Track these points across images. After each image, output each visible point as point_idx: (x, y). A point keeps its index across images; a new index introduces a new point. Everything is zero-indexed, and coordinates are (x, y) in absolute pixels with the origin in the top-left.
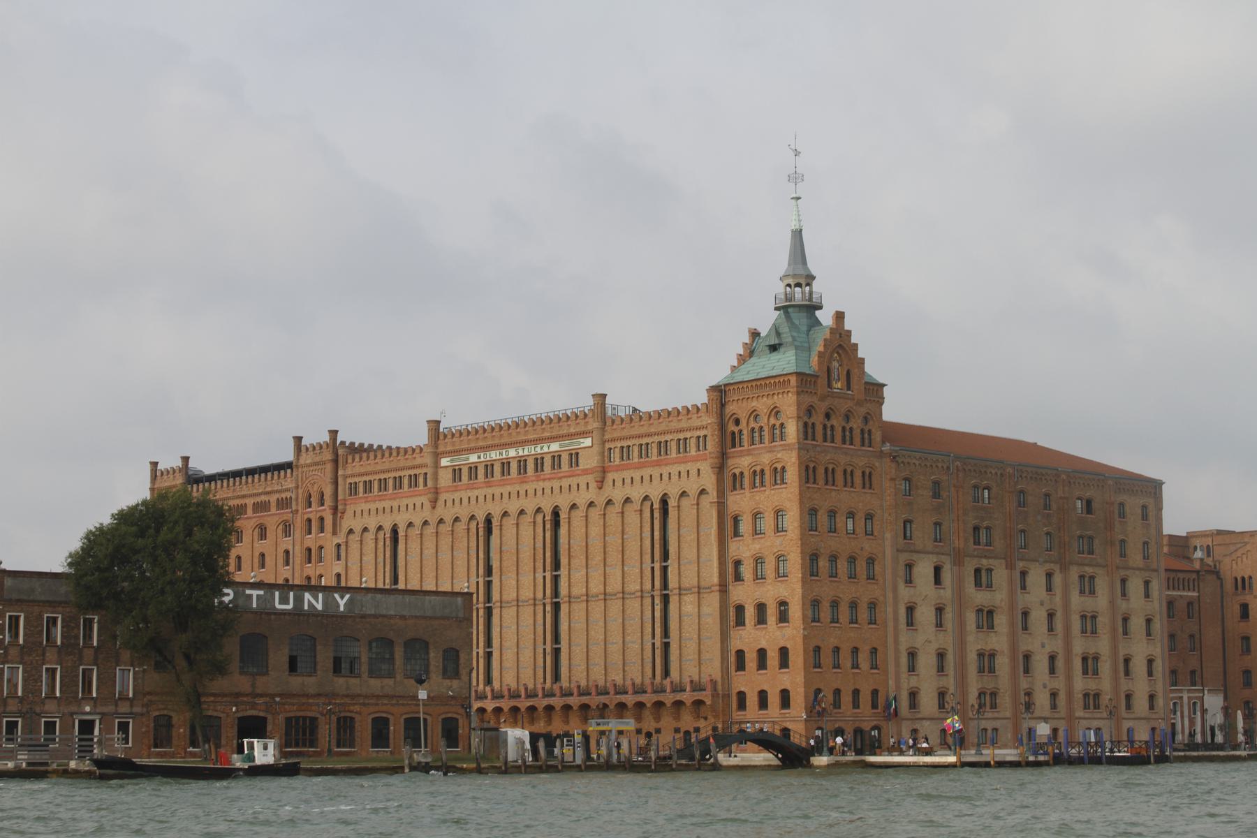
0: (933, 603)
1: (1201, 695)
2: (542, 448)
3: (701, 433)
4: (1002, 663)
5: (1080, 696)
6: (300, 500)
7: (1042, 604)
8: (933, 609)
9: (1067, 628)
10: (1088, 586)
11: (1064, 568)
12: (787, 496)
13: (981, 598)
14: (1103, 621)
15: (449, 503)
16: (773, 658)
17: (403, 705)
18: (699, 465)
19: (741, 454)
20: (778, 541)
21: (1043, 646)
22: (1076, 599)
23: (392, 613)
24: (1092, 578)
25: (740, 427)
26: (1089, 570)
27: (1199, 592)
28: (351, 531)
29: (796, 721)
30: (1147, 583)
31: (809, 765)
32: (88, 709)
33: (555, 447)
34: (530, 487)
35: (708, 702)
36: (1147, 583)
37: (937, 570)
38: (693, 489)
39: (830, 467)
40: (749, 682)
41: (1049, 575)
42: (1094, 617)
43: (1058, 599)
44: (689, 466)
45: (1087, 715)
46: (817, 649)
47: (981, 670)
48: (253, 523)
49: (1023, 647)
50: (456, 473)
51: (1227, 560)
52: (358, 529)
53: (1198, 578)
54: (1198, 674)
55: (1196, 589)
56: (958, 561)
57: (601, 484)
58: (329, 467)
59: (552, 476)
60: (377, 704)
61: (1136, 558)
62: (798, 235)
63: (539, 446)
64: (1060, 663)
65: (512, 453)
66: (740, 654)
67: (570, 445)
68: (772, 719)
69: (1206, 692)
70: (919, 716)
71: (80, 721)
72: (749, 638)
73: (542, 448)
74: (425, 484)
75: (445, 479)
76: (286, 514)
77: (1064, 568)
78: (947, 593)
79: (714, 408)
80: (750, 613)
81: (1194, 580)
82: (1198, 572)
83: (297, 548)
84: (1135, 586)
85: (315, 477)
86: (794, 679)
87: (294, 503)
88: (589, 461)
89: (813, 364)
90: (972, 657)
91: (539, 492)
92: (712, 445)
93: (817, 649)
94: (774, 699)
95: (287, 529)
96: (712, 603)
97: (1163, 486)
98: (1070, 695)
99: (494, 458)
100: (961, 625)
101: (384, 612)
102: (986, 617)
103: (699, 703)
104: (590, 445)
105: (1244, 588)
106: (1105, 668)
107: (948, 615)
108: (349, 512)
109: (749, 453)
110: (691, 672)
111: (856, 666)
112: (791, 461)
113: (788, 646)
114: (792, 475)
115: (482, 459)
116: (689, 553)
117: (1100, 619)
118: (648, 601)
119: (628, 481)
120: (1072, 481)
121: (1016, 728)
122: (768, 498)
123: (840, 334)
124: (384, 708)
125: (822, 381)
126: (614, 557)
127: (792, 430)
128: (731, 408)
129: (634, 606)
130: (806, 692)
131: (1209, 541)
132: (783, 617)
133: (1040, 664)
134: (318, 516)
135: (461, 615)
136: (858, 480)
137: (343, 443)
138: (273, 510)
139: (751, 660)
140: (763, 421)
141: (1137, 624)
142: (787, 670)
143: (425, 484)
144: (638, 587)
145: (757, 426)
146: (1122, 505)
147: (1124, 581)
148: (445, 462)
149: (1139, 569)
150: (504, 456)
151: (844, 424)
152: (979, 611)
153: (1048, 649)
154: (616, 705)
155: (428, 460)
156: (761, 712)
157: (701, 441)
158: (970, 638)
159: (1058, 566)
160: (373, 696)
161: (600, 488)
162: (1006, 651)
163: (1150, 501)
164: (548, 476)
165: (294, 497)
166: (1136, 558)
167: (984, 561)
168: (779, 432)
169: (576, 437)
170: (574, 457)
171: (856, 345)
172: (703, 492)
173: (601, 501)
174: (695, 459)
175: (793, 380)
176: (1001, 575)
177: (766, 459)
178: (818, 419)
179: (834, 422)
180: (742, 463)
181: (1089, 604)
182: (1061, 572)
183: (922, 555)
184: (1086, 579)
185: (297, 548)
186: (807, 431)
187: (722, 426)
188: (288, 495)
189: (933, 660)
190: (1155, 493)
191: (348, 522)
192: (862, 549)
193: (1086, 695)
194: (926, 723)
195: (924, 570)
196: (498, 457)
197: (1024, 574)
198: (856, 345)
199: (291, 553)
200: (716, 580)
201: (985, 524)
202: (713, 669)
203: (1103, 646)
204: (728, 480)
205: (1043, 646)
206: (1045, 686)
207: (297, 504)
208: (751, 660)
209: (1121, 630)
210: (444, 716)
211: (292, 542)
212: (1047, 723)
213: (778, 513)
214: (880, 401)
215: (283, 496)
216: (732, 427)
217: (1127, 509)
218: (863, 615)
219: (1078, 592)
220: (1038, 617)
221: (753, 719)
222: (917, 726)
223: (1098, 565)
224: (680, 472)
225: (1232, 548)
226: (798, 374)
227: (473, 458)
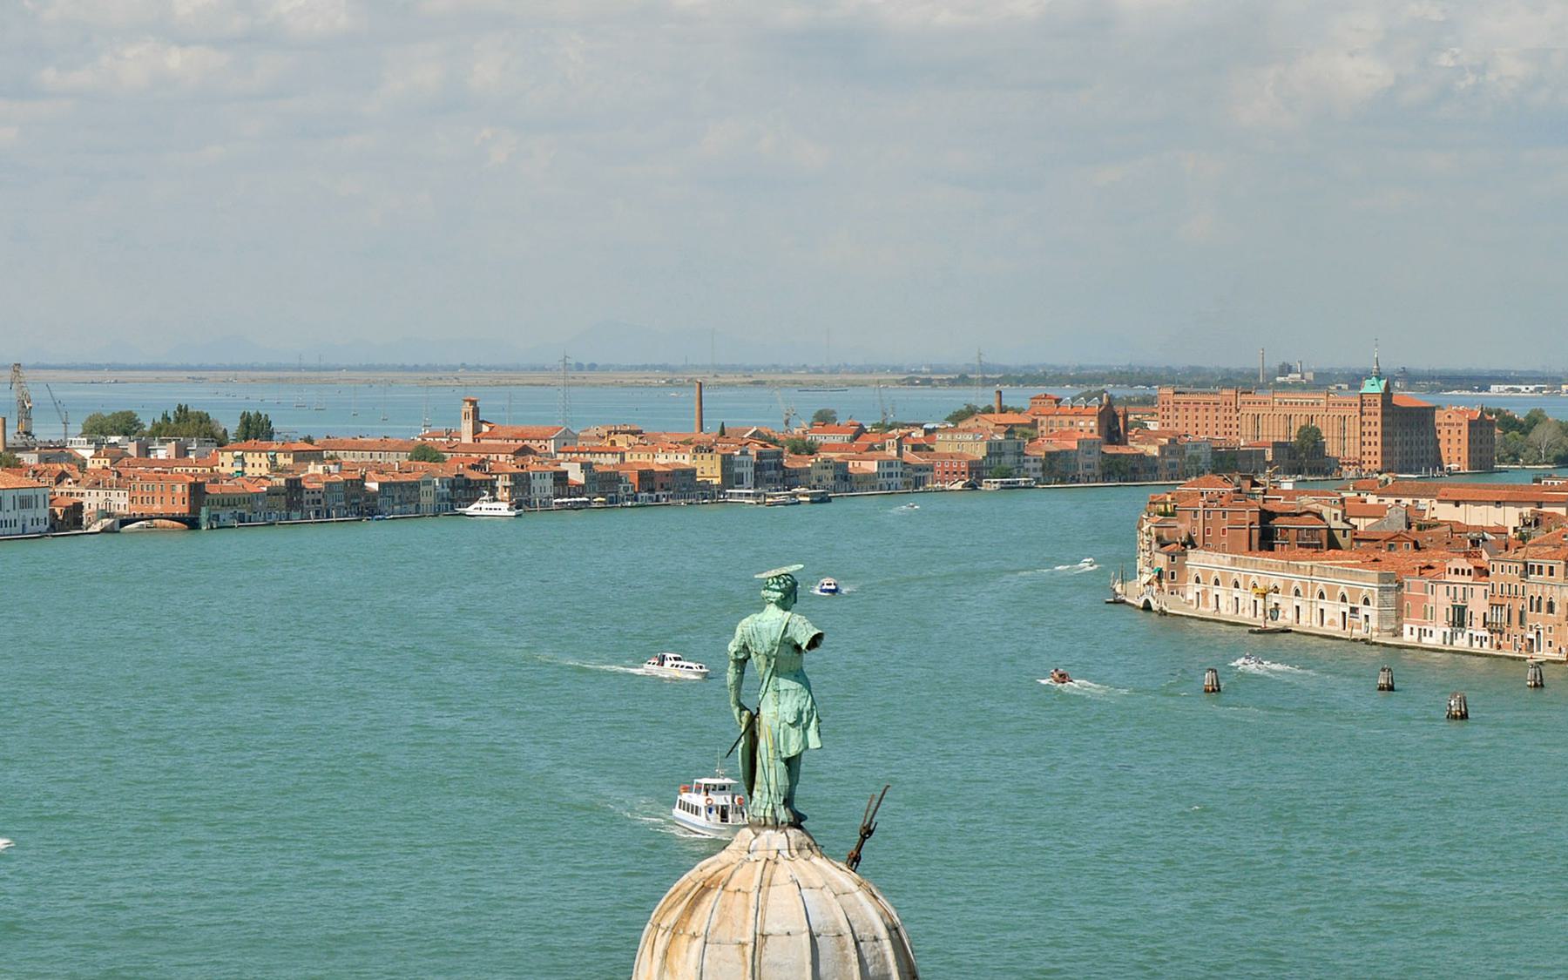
12: (1378, 419)
50: (1280, 403)
52: (1245, 413)
75: (1276, 404)
92: (1359, 406)
94: (1373, 462)
114: (1379, 414)
122: (1372, 419)
127: (1379, 405)
129: (1335, 440)
168: (1376, 405)
204: (1362, 414)
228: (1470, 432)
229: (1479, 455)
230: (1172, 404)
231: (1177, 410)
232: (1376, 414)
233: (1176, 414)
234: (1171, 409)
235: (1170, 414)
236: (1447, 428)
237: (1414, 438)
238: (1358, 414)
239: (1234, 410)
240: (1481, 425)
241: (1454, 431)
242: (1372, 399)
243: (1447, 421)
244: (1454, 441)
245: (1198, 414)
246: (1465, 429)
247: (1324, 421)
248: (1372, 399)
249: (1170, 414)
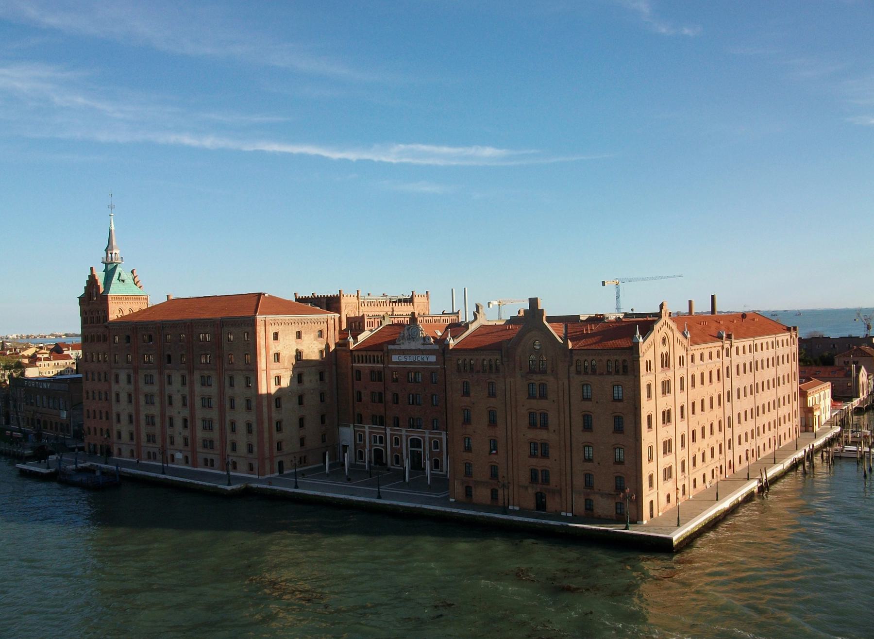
5: (201, 441)
10: (205, 382)
11: (191, 373)
13: (147, 389)
21: (179, 413)
22: (198, 388)
24: (209, 377)
37: (129, 376)
41: (183, 377)
47: (148, 424)
62: (110, 231)
90: (142, 417)
100: (137, 403)
147: (231, 378)
149: (241, 370)
152: (146, 395)
181: (207, 391)
189: (127, 418)
195: (123, 377)
197: (169, 377)
205: (179, 413)
206: (180, 434)
212: (181, 452)
219: (199, 385)
220: (177, 399)
222: (120, 447)
237: (176, 388)
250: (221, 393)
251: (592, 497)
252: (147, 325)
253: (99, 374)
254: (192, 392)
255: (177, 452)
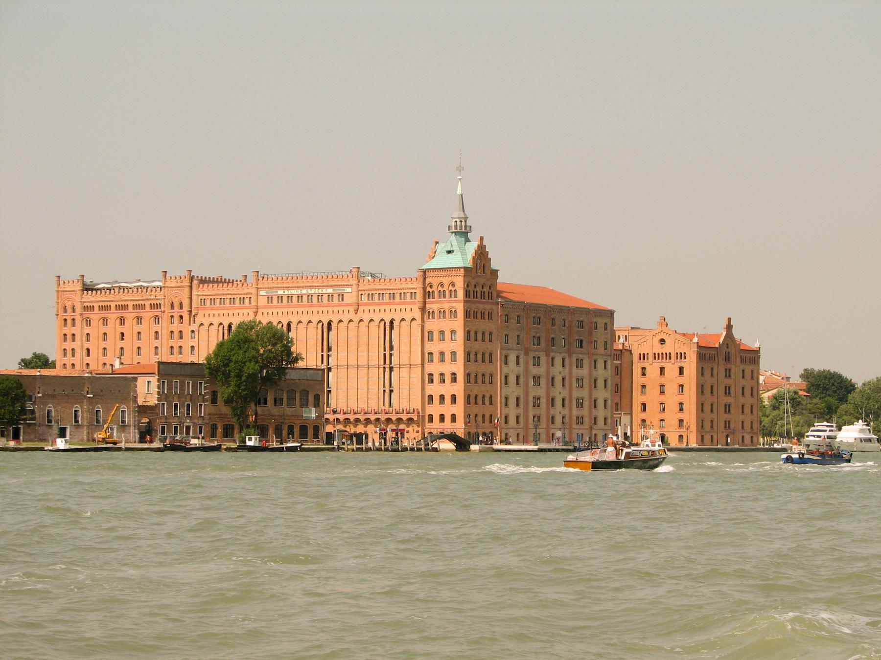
0: (516, 373)
1: (620, 416)
2: (322, 291)
3: (413, 291)
4: (543, 401)
6: (166, 305)
7: (560, 373)
8: (515, 376)
9: (571, 384)
11: (570, 355)
12: (458, 324)
13: (534, 371)
14: (586, 381)
15: (265, 314)
16: (448, 399)
17: (299, 419)
18: (412, 306)
19: (432, 303)
20: (452, 345)
21: (560, 393)
22: (574, 370)
23: (295, 378)
24: (582, 360)
25: (433, 290)
26: (581, 356)
27: (621, 361)
28: (202, 324)
29: (459, 429)
30: (605, 362)
31: (468, 450)
32: (188, 421)
33: (330, 291)
34: (315, 310)
35: (415, 419)
36: (605, 362)
38: (408, 318)
39: (476, 310)
40: (434, 410)
42: (582, 380)
43: (567, 370)
44: (406, 306)
45: (577, 427)
46: (469, 396)
48: (134, 315)
49: (551, 395)
50: (270, 299)
51: (636, 344)
53: (621, 354)
54: (619, 405)
55: (620, 359)
56: (526, 354)
57: (356, 311)
58: (187, 290)
59: (328, 305)
60: (289, 419)
61: (601, 349)
63: (321, 290)
64: (567, 402)
65: (304, 291)
66: (431, 397)
67: (339, 290)
68: (448, 427)
69: (622, 414)
70: (509, 427)
71: (186, 426)
72: (435, 389)
73: (322, 291)
74: (250, 303)
76: (157, 312)
77: (570, 355)
78: (521, 369)
79: (421, 279)
80: (436, 378)
81: (619, 355)
82: (621, 350)
83: (164, 331)
84: (600, 364)
85: (179, 294)
86: (459, 409)
87: (162, 307)
88: (350, 299)
89: (469, 263)
90: (531, 399)
91: (320, 312)
92: (419, 297)
93: (469, 396)
94: (448, 418)
95: (157, 319)
96: (417, 373)
97: (615, 313)
98: (571, 417)
99: (293, 293)
101: (292, 378)
102: (537, 379)
103: (410, 420)
104: (351, 291)
105: (644, 359)
106: (586, 404)
107: (522, 380)
108: (201, 313)
109: (437, 302)
110: (405, 405)
111: (484, 403)
112: (460, 308)
113: (456, 394)
114: (461, 314)
115: (286, 293)
116: (405, 348)
117: (584, 380)
118: (382, 370)
119: (372, 311)
120: (575, 312)
121: (548, 432)
122: (447, 324)
123: (482, 247)
124: (293, 421)
125: (474, 271)
126: (363, 347)
127: (461, 294)
128: (428, 281)
129: (374, 372)
130: (464, 415)
131: (626, 333)
132: (454, 380)
133: (558, 402)
134: (178, 315)
135: (320, 379)
136: (486, 316)
137: (193, 276)
138: (148, 308)
139: (436, 399)
140: (446, 288)
141: (600, 383)
142: (455, 405)
143: (250, 303)
144: (377, 363)
145: (442, 290)
146: (596, 323)
147: (595, 361)
148: (262, 293)
149: (602, 355)
150: (299, 293)
151: (481, 289)
152: (534, 377)
153: (562, 396)
154: (385, 419)
155: (254, 291)
156: (441, 424)
157: (413, 295)
158: (530, 390)
159: (567, 355)
160: (293, 416)
161: (356, 313)
162: (545, 397)
163: (608, 321)
164: (326, 305)
165: (162, 303)
166: (601, 349)
167: (537, 353)
169: (344, 287)
170: (341, 296)
171: (488, 252)
172: (413, 319)
173: (356, 319)
174: (409, 303)
175: (462, 270)
176: (543, 360)
177: (447, 306)
178: (471, 288)
179: (477, 289)
180: (432, 306)
182: (569, 357)
183: (511, 351)
184: (579, 361)
185: (164, 331)
186: (467, 294)
187: (424, 289)
188: (158, 302)
190: (611, 317)
191: (198, 320)
192: (487, 348)
193: (578, 418)
194: (512, 430)
195: (512, 358)
196: (296, 293)
198: (488, 252)
199: (160, 333)
200: (420, 362)
201: (538, 335)
202: (417, 404)
203: (584, 393)
205: (560, 393)
206: (560, 413)
207: (165, 307)
208: (436, 399)
209: (593, 385)
210: (314, 425)
211: (160, 327)
213: (453, 332)
214: (496, 277)
215: (155, 302)
216: (428, 289)
217: (598, 325)
218: (487, 380)
221: (436, 427)
223: (584, 354)
224: (401, 309)
225: (640, 338)
226: (464, 268)
227: (280, 292)
228: (701, 372)
229: (724, 417)
230: (79, 310)
231: (89, 322)
232: (454, 313)
233: (87, 330)
234: (78, 322)
235: (76, 330)
236: (658, 364)
238: (417, 314)
239: (186, 317)
240: (727, 359)
241: (671, 369)
242: (446, 281)
243: (659, 349)
244: (671, 389)
245: (142, 328)
246: (691, 365)
247: (353, 333)
248: (446, 281)
249: (76, 330)
250: (590, 374)
251: (744, 435)
252: (539, 307)
253: (483, 355)
254: (571, 373)
255: (557, 431)
